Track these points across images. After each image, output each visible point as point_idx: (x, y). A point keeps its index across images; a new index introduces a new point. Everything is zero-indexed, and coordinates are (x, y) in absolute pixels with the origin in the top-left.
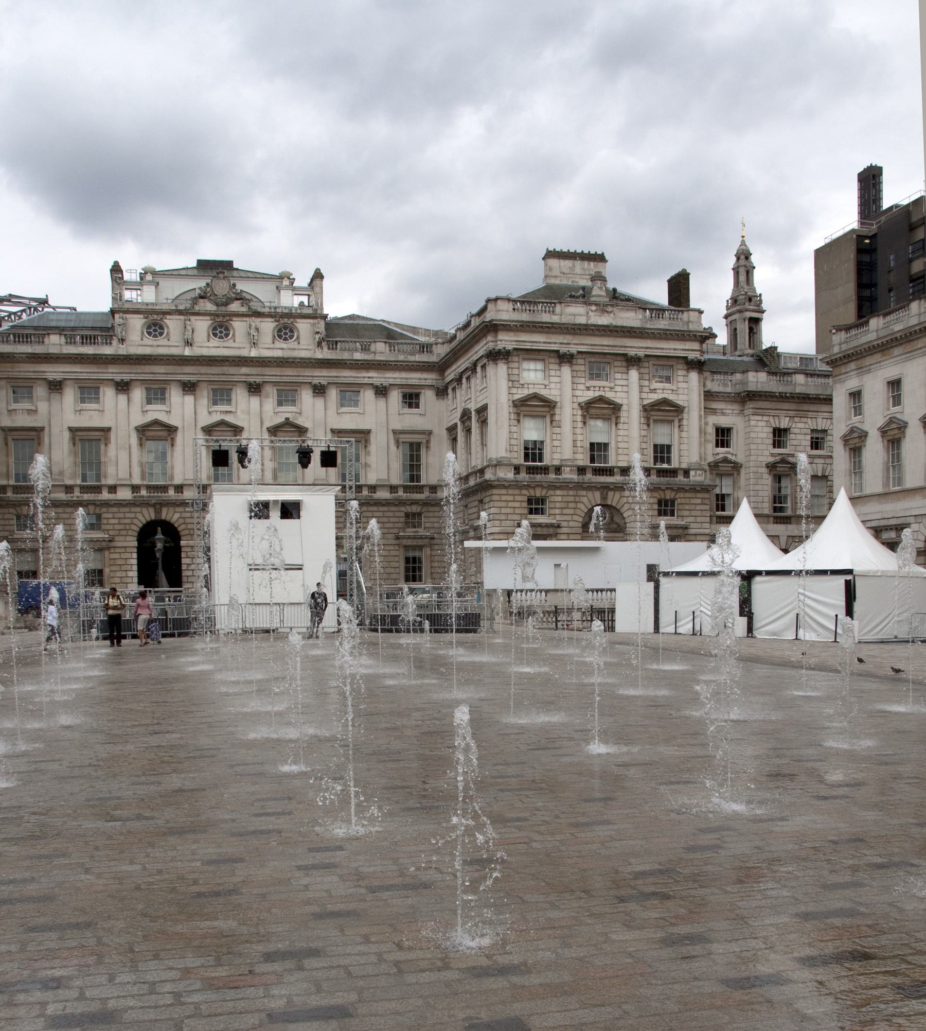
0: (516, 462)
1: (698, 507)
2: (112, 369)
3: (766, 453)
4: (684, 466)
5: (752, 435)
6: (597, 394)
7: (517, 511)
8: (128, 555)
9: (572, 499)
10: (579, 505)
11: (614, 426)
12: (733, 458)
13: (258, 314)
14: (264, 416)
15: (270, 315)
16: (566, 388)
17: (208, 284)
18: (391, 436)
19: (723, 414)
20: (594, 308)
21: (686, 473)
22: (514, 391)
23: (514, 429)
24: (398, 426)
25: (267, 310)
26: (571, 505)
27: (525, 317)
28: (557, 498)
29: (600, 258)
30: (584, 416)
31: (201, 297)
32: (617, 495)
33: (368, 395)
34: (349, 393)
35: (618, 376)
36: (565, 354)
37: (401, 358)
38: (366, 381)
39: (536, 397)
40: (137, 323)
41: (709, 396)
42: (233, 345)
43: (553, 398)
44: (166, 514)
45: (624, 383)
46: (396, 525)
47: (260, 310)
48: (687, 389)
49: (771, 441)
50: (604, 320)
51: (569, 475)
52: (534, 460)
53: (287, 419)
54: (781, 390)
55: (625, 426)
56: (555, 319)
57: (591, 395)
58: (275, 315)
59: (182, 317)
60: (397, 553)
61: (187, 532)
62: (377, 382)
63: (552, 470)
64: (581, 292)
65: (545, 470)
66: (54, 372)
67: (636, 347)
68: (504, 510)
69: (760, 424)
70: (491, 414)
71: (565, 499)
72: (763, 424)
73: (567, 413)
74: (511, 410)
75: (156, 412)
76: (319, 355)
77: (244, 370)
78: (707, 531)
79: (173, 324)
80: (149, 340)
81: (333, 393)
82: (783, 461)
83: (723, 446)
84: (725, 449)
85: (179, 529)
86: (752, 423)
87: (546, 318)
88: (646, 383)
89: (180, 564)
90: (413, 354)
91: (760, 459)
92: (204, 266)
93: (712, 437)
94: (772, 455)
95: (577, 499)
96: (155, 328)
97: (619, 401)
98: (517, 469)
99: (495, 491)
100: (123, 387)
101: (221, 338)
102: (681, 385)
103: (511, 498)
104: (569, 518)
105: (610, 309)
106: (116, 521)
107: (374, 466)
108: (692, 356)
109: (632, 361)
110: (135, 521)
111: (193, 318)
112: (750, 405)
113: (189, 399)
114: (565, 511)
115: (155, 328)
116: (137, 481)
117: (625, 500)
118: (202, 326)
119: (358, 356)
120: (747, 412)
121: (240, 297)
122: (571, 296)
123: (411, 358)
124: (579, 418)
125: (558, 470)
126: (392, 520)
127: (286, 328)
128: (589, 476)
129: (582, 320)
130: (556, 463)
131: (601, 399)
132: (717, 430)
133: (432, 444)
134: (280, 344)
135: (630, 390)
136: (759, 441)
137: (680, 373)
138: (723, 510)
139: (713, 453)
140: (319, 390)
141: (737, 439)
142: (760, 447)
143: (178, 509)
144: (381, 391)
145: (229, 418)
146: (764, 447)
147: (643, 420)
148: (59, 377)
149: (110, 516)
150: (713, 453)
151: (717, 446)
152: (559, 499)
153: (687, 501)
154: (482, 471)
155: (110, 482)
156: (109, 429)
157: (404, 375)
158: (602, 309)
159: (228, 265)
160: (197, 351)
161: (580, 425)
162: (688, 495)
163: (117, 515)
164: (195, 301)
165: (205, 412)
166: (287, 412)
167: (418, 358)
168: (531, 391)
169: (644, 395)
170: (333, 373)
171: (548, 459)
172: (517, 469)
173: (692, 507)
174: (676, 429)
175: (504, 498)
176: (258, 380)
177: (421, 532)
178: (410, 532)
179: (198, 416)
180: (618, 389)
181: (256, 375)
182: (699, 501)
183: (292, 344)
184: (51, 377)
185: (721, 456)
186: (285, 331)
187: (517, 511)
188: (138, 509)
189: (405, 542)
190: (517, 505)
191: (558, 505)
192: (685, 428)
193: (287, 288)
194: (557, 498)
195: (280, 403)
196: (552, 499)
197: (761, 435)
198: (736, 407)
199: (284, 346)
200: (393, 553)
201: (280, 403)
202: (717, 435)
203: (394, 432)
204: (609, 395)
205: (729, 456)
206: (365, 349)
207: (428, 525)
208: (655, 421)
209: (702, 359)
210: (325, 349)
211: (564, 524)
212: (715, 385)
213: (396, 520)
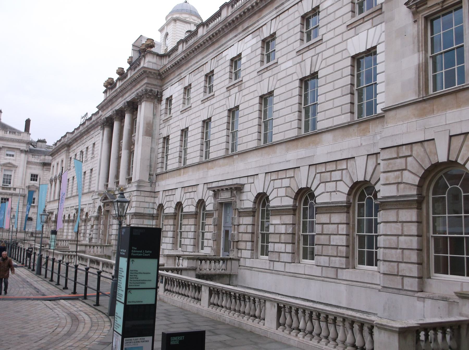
4: (15, 187)
5: (45, 178)
21: (15, 189)
41: (28, 163)
48: (20, 160)
83: (34, 180)
84: (35, 182)
86: (45, 173)
88: (3, 156)
93: (29, 177)
108: (22, 148)
112: (45, 167)
120: (44, 169)
138: (34, 203)
151: (31, 180)
185: (32, 184)
198: (41, 167)
205: (35, 185)
212: (32, 159)
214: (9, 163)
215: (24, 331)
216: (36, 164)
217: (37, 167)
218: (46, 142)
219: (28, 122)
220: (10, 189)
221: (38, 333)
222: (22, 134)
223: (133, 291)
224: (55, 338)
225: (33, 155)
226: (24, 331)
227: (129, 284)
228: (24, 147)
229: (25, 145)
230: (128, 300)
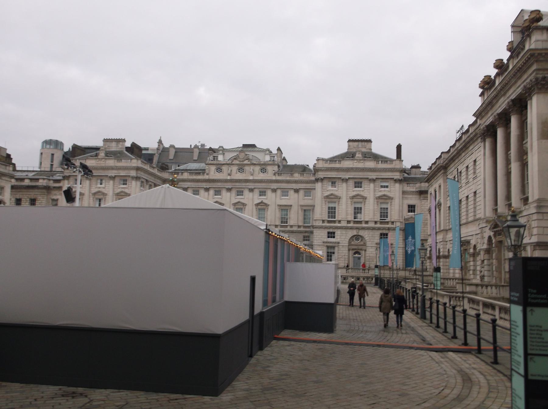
4: (392, 220)
13: (255, 164)
18: (300, 207)
20: (356, 161)
22: (324, 193)
29: (370, 141)
30: (351, 202)
33: (292, 192)
34: (285, 192)
35: (366, 186)
40: (213, 168)
41: (404, 193)
43: (339, 195)
45: (368, 189)
48: (395, 190)
57: (355, 193)
62: (295, 188)
63: (337, 222)
74: (323, 200)
76: (274, 178)
79: (224, 168)
81: (279, 192)
86: (423, 203)
87: (337, 165)
88: (377, 188)
92: (245, 146)
93: (406, 208)
97: (365, 196)
98: (323, 221)
108: (395, 177)
111: (232, 166)
112: (422, 196)
113: (229, 194)
114: (342, 237)
115: (219, 170)
118: (235, 169)
120: (422, 198)
129: (351, 166)
130: (340, 219)
135: (369, 191)
140: (274, 191)
144: (297, 191)
145: (242, 201)
148: (186, 186)
151: (409, 212)
157: (305, 185)
159: (253, 146)
170: (279, 185)
181: (251, 185)
186: (264, 170)
194: (338, 233)
198: (417, 196)
202: (409, 208)
203: (302, 206)
211: (341, 242)
214: (384, 195)
215: (405, 388)
216: (412, 193)
217: (414, 196)
218: (420, 168)
219: (399, 148)
220: (387, 223)
221: (421, 393)
222: (394, 162)
223: (536, 358)
224: (442, 401)
225: (408, 184)
226: (405, 388)
227: (529, 347)
228: (397, 176)
229: (398, 174)
230: (531, 371)
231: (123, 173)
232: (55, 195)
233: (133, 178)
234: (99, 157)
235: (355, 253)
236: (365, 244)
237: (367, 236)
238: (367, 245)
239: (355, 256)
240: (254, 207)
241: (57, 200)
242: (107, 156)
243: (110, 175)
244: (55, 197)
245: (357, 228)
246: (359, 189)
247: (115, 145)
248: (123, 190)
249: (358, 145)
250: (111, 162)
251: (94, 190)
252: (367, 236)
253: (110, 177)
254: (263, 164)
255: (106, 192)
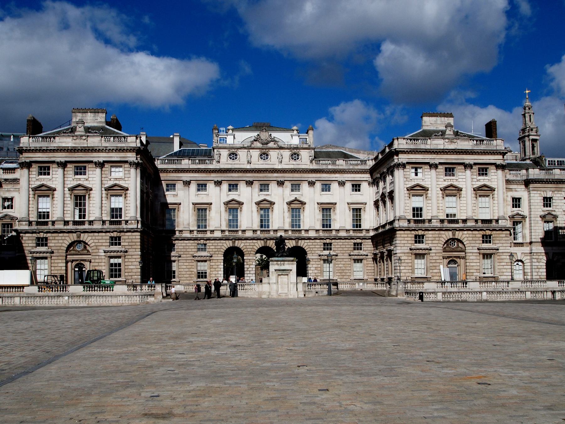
0: (409, 218)
1: (504, 239)
2: (213, 175)
3: (539, 209)
4: (496, 218)
6: (449, 183)
7: (409, 242)
8: (219, 264)
9: (437, 236)
10: (441, 239)
11: (458, 199)
12: (522, 213)
13: (281, 148)
14: (284, 196)
15: (287, 149)
16: (432, 179)
17: (258, 135)
19: (516, 191)
20: (447, 140)
21: (497, 221)
22: (407, 183)
23: (407, 201)
24: (350, 201)
25: (286, 146)
26: (437, 239)
27: (412, 147)
28: (429, 235)
31: (255, 141)
32: (461, 233)
35: (460, 174)
36: (433, 164)
37: (351, 167)
38: (334, 179)
39: (418, 185)
40: (225, 153)
41: (508, 182)
42: (270, 163)
44: (238, 244)
45: (464, 177)
46: (350, 249)
47: (283, 146)
48: (496, 178)
49: (543, 204)
50: (452, 146)
51: (436, 224)
52: (418, 217)
53: (296, 198)
54: (547, 178)
55: (465, 199)
56: (428, 147)
58: (289, 148)
59: (246, 150)
60: (350, 263)
61: (247, 252)
62: (340, 179)
64: (440, 133)
65: (423, 221)
66: (186, 177)
67: (469, 159)
68: (402, 242)
69: (536, 195)
70: (396, 195)
71: (434, 236)
72: (538, 195)
73: (435, 193)
75: (233, 195)
77: (275, 175)
78: (508, 251)
79: (242, 154)
80: (230, 161)
82: (549, 214)
83: (516, 207)
84: (518, 209)
85: (244, 251)
87: (423, 147)
88: (475, 177)
89: (244, 268)
90: (357, 165)
91: (537, 213)
94: (543, 211)
95: (440, 236)
96: (233, 155)
98: (409, 221)
99: (398, 232)
100: (218, 183)
101: (264, 159)
102: (493, 177)
103: (406, 236)
104: (436, 245)
105: (455, 141)
106: (213, 247)
107: (338, 220)
108: (498, 162)
109: (467, 166)
110: (223, 247)
111: (251, 150)
113: (249, 189)
114: (434, 242)
115: (233, 155)
116: (224, 228)
117: (465, 236)
118: (255, 154)
119: (330, 167)
121: (274, 140)
122: (435, 135)
123: (356, 167)
124: (441, 195)
125: (430, 221)
126: (347, 246)
127: (295, 154)
128: (446, 224)
131: (451, 186)
132: (513, 199)
133: (367, 209)
134: (293, 162)
136: (536, 204)
137: (492, 171)
139: (510, 210)
141: (524, 203)
142: (537, 207)
143: (243, 241)
145: (268, 198)
146: (539, 207)
147: (473, 195)
148: (188, 179)
149: (211, 244)
150: (510, 210)
151: (513, 207)
152: (431, 236)
153: (498, 236)
154: (391, 223)
155: (212, 228)
156: (211, 204)
157: (353, 175)
158: (451, 141)
160: (252, 166)
161: (441, 198)
162: (498, 232)
163: (214, 244)
164: (252, 142)
165: (257, 195)
166: (296, 195)
167: (359, 167)
168: (416, 183)
169: (474, 183)
170: (318, 175)
171: (426, 215)
172: (409, 221)
173: (501, 239)
174: (491, 199)
175: (402, 236)
176: (282, 179)
177: (362, 252)
178: (356, 252)
179: (253, 197)
180: (460, 180)
181: (281, 176)
182: (504, 235)
183: (298, 162)
184: (185, 179)
185: (515, 212)
186: (295, 156)
187: (409, 242)
188: (224, 241)
189: (353, 257)
190: (410, 239)
191: (430, 239)
192: (496, 199)
193: (295, 135)
195: (292, 190)
196: (427, 236)
197: (536, 201)
199: (294, 163)
200: (348, 263)
201: (292, 190)
202: (513, 202)
204: (455, 183)
205: (520, 212)
206: (334, 164)
207: (365, 249)
208: (480, 196)
209: (504, 164)
210: (314, 164)
213: (349, 246)
217: (519, 187)
231: (115, 156)
232: (9, 191)
233: (131, 164)
234: (76, 134)
235: (449, 263)
236: (464, 251)
237: (466, 239)
238: (467, 251)
239: (449, 266)
240: (286, 207)
241: (11, 199)
242: (89, 132)
243: (95, 160)
244: (9, 195)
245: (455, 230)
246: (452, 178)
247: (92, 118)
248: (117, 182)
249: (436, 121)
250: (94, 141)
251: (71, 183)
252: (466, 239)
253: (96, 163)
254: (294, 148)
255: (90, 186)
